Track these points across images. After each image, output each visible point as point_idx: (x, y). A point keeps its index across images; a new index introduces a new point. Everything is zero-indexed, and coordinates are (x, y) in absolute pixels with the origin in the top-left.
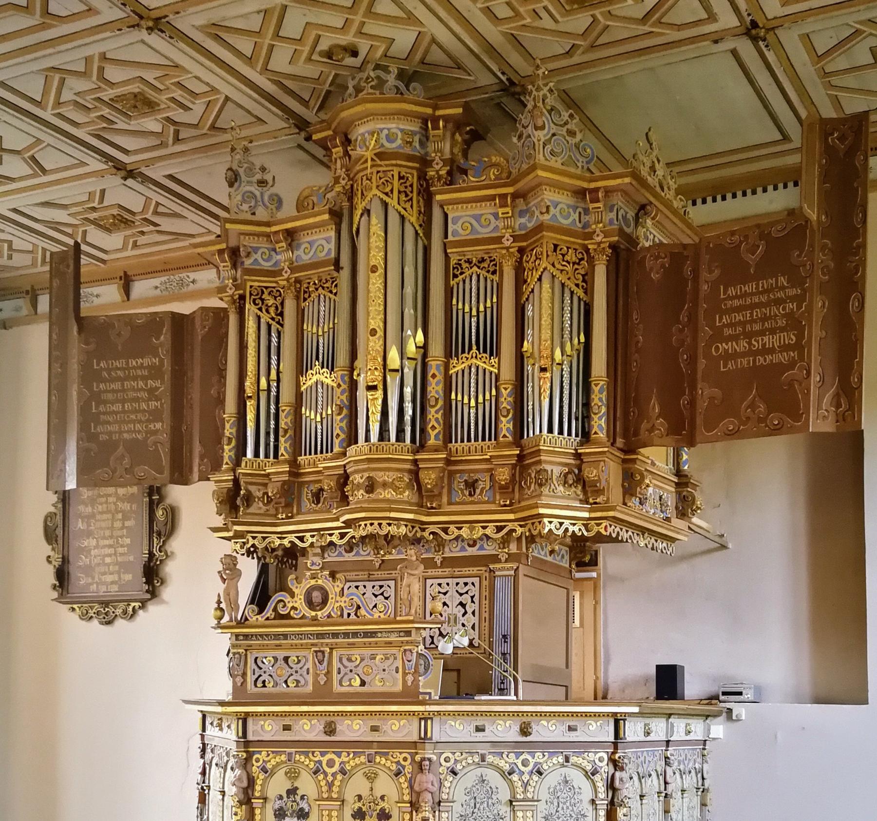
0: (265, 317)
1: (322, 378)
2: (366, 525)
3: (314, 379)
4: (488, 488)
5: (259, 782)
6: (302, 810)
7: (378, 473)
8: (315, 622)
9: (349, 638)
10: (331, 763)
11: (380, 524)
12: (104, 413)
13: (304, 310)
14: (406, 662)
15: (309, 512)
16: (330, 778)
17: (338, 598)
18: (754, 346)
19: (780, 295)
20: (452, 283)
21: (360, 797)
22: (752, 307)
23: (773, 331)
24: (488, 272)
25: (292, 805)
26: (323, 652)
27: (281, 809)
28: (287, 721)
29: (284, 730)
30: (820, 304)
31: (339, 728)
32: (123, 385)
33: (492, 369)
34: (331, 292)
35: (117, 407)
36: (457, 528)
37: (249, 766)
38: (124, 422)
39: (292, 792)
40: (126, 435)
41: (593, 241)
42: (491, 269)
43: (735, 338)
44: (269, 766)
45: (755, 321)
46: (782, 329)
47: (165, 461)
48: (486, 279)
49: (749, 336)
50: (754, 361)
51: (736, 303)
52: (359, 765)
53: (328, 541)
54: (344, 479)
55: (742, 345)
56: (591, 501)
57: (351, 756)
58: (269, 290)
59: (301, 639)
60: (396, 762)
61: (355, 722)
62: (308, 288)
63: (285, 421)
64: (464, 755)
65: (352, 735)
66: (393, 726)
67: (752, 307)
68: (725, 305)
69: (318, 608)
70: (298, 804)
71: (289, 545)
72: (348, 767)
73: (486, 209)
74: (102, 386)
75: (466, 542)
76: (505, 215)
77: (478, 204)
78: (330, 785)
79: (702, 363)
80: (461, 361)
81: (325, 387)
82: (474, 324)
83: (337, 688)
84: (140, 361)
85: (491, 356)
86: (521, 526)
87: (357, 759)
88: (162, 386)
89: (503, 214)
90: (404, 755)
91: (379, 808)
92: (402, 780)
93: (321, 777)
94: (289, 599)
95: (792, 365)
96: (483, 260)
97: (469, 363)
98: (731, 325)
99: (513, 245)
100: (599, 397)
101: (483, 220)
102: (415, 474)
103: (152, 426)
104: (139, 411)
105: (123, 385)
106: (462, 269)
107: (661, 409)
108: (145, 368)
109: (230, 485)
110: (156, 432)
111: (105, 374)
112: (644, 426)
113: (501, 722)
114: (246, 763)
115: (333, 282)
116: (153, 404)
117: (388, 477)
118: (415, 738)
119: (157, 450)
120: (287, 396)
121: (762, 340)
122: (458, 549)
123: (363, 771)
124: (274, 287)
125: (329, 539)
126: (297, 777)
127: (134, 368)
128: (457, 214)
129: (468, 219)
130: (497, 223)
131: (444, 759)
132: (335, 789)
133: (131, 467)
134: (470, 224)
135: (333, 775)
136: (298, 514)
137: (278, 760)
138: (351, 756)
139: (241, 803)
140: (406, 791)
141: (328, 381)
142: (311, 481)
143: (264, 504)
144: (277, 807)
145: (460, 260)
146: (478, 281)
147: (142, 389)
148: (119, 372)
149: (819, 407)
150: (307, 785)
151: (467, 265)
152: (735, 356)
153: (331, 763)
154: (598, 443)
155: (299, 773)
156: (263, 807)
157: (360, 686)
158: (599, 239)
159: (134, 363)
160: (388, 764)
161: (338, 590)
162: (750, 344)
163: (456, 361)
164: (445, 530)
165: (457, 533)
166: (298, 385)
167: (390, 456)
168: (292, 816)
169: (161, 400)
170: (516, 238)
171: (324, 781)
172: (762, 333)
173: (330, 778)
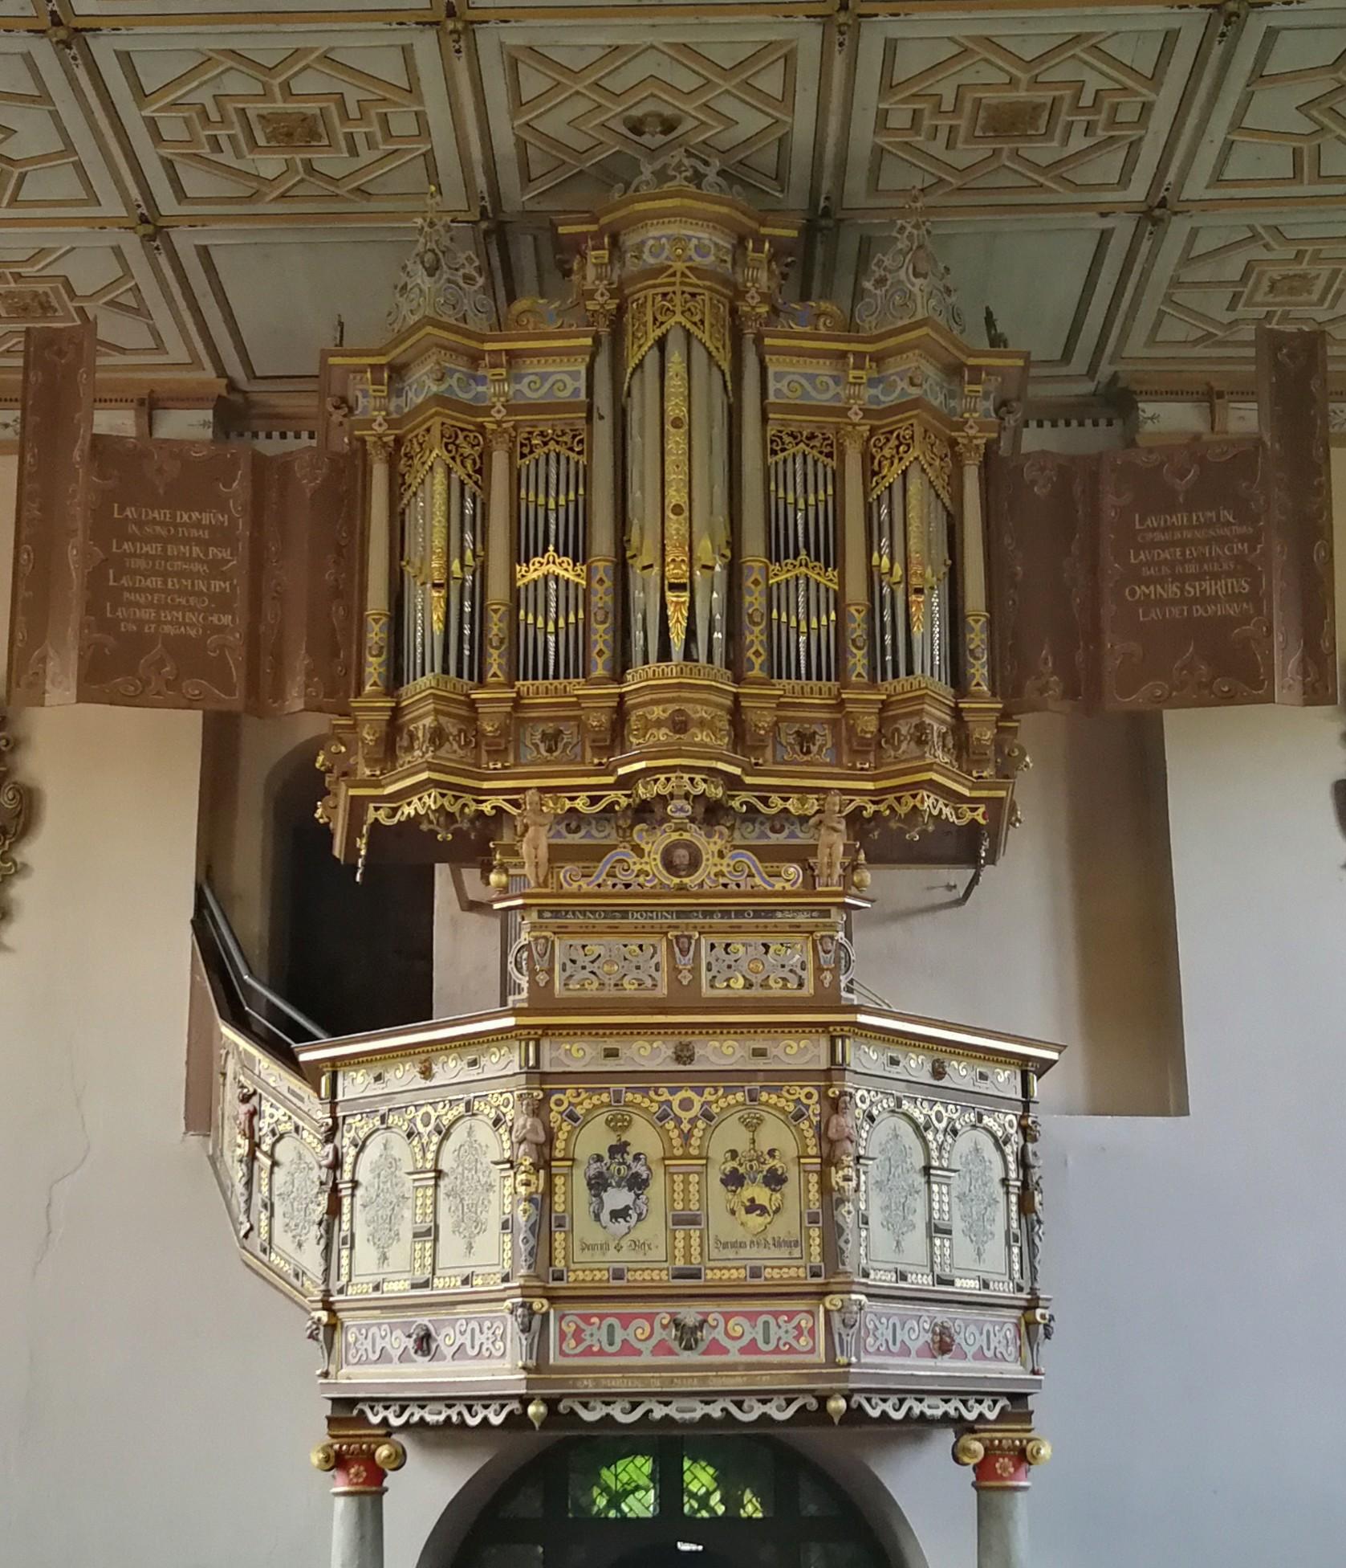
0: (459, 472)
1: (552, 568)
2: (668, 780)
3: (544, 569)
4: (829, 745)
5: (562, 1136)
6: (637, 1175)
7: (691, 705)
8: (683, 892)
9: (730, 918)
10: (686, 1104)
11: (692, 780)
12: (129, 589)
13: (519, 471)
14: (822, 954)
15: (532, 763)
16: (686, 1127)
17: (717, 860)
18: (1189, 592)
19: (1226, 531)
20: (770, 460)
21: (734, 1154)
22: (1183, 544)
23: (1215, 576)
24: (821, 453)
25: (619, 1170)
26: (690, 938)
27: (600, 1175)
28: (611, 1043)
29: (607, 1056)
30: (1279, 552)
31: (699, 1051)
32: (164, 550)
33: (829, 584)
34: (571, 449)
35: (155, 582)
36: (782, 798)
37: (543, 1113)
38: (163, 606)
39: (619, 1149)
40: (167, 629)
41: (964, 434)
42: (826, 450)
43: (1160, 580)
44: (579, 1111)
45: (1190, 561)
46: (1229, 574)
47: (237, 675)
48: (815, 462)
49: (1182, 579)
50: (1190, 611)
51: (1159, 537)
52: (734, 1106)
53: (567, 807)
54: (621, 712)
55: (1173, 589)
56: (975, 774)
57: (721, 1092)
58: (466, 433)
59: (651, 918)
60: (793, 1101)
61: (726, 1044)
62: (528, 439)
63: (496, 627)
64: (880, 1096)
65: (723, 1062)
66: (788, 1050)
67: (1183, 544)
68: (1143, 538)
69: (683, 873)
70: (629, 1167)
71: (494, 812)
72: (715, 1109)
73: (823, 369)
74: (127, 546)
75: (768, 825)
76: (859, 381)
77: (814, 361)
78: (687, 1137)
79: (1109, 610)
80: (785, 569)
81: (562, 584)
82: (800, 522)
83: (706, 991)
84: (195, 515)
85: (827, 565)
86: (874, 802)
87: (731, 1097)
88: (234, 560)
89: (854, 378)
90: (806, 1090)
91: (766, 1167)
92: (805, 1125)
93: (670, 1125)
94: (636, 859)
95: (1245, 619)
96: (812, 437)
97: (797, 571)
98: (1148, 564)
99: (863, 421)
100: (977, 637)
101: (818, 382)
102: (736, 712)
103: (215, 619)
104: (193, 593)
105: (164, 550)
106: (783, 443)
107: (1054, 663)
108: (204, 527)
109: (386, 716)
110: (221, 629)
111: (133, 528)
112: (1029, 684)
113: (913, 1056)
114: (538, 1110)
115: (574, 437)
116: (217, 585)
117: (701, 712)
118: (824, 1064)
119: (222, 657)
120: (498, 591)
121: (1201, 586)
122: (754, 835)
123: (741, 1114)
124: (470, 431)
125: (568, 805)
126: (627, 1127)
127: (184, 525)
128: (778, 369)
129: (796, 377)
130: (839, 389)
131: (863, 1097)
132: (695, 1142)
133: (176, 679)
134: (802, 386)
135: (693, 1121)
136: (515, 765)
137: (595, 1100)
138: (721, 1092)
139: (536, 1167)
140: (812, 1142)
141: (570, 575)
142: (539, 719)
143: (460, 747)
144: (592, 1172)
145: (781, 432)
146: (805, 462)
147: (198, 559)
148: (158, 528)
149: (1284, 674)
150: (644, 1138)
151: (791, 439)
152: (1161, 602)
153: (686, 1104)
154: (978, 696)
155: (630, 1121)
156: (568, 1176)
157: (745, 987)
158: (972, 432)
159: (185, 517)
160: (782, 1103)
161: (716, 849)
162: (1182, 590)
163: (778, 567)
164: (765, 801)
165: (781, 805)
166: (512, 578)
167: (713, 683)
168: (619, 1185)
169: (231, 580)
170: (867, 413)
171: (676, 1132)
172: (1199, 577)
173: (686, 1127)
